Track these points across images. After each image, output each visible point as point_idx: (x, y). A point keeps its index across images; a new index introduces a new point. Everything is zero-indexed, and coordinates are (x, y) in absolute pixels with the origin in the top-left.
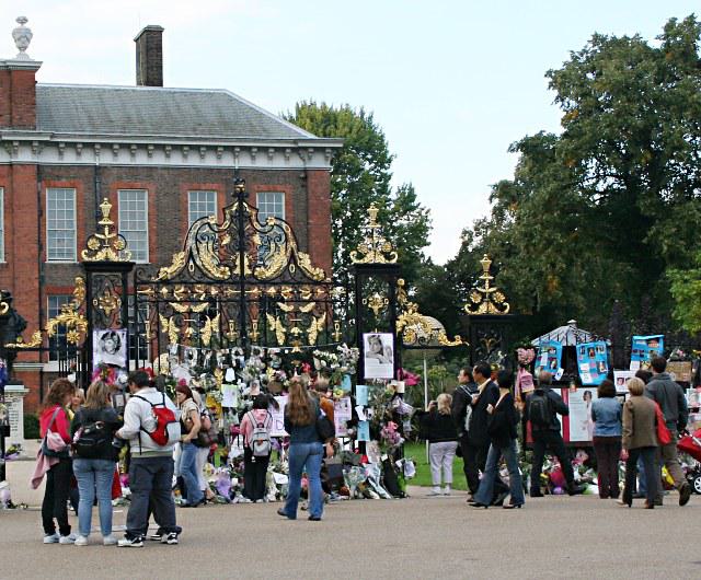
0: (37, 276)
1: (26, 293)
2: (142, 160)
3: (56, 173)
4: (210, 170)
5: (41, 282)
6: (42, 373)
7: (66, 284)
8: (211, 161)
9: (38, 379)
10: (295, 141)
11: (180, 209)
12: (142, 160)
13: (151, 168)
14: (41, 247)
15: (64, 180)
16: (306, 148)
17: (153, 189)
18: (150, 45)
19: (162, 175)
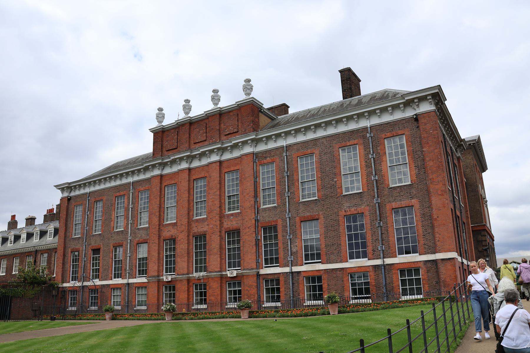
0: (254, 216)
1: (249, 228)
2: (311, 136)
3: (264, 156)
4: (352, 132)
5: (257, 221)
6: (258, 275)
7: (271, 219)
8: (352, 126)
9: (255, 278)
10: (403, 96)
11: (335, 161)
12: (311, 136)
13: (315, 140)
15: (268, 158)
16: (412, 101)
17: (317, 152)
18: (349, 81)
19: (323, 143)
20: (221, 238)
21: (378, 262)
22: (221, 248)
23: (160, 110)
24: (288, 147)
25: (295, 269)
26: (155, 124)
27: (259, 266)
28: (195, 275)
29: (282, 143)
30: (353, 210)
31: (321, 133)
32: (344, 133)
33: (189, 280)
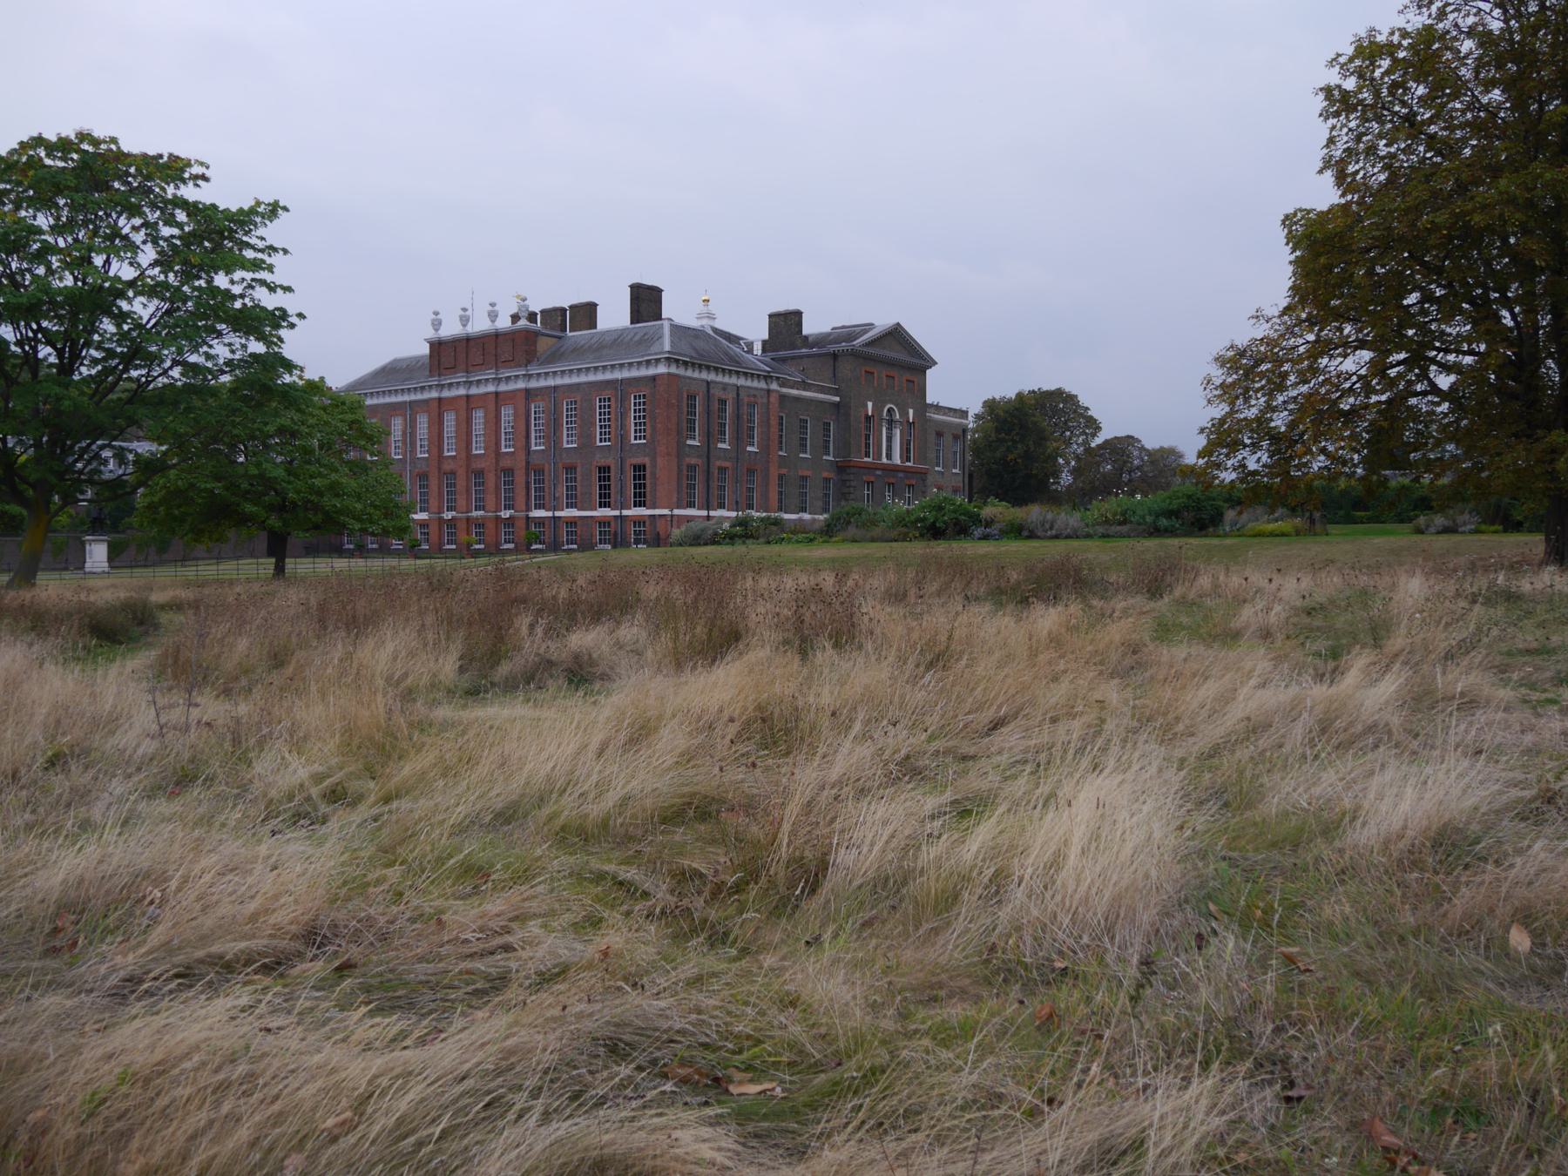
5: (528, 463)
6: (528, 518)
14: (528, 437)
20: (498, 478)
21: (617, 513)
22: (497, 488)
23: (436, 313)
24: (555, 387)
25: (558, 514)
26: (431, 334)
27: (528, 509)
28: (475, 514)
29: (551, 382)
30: (603, 463)
31: (583, 379)
32: (602, 382)
33: (468, 519)
